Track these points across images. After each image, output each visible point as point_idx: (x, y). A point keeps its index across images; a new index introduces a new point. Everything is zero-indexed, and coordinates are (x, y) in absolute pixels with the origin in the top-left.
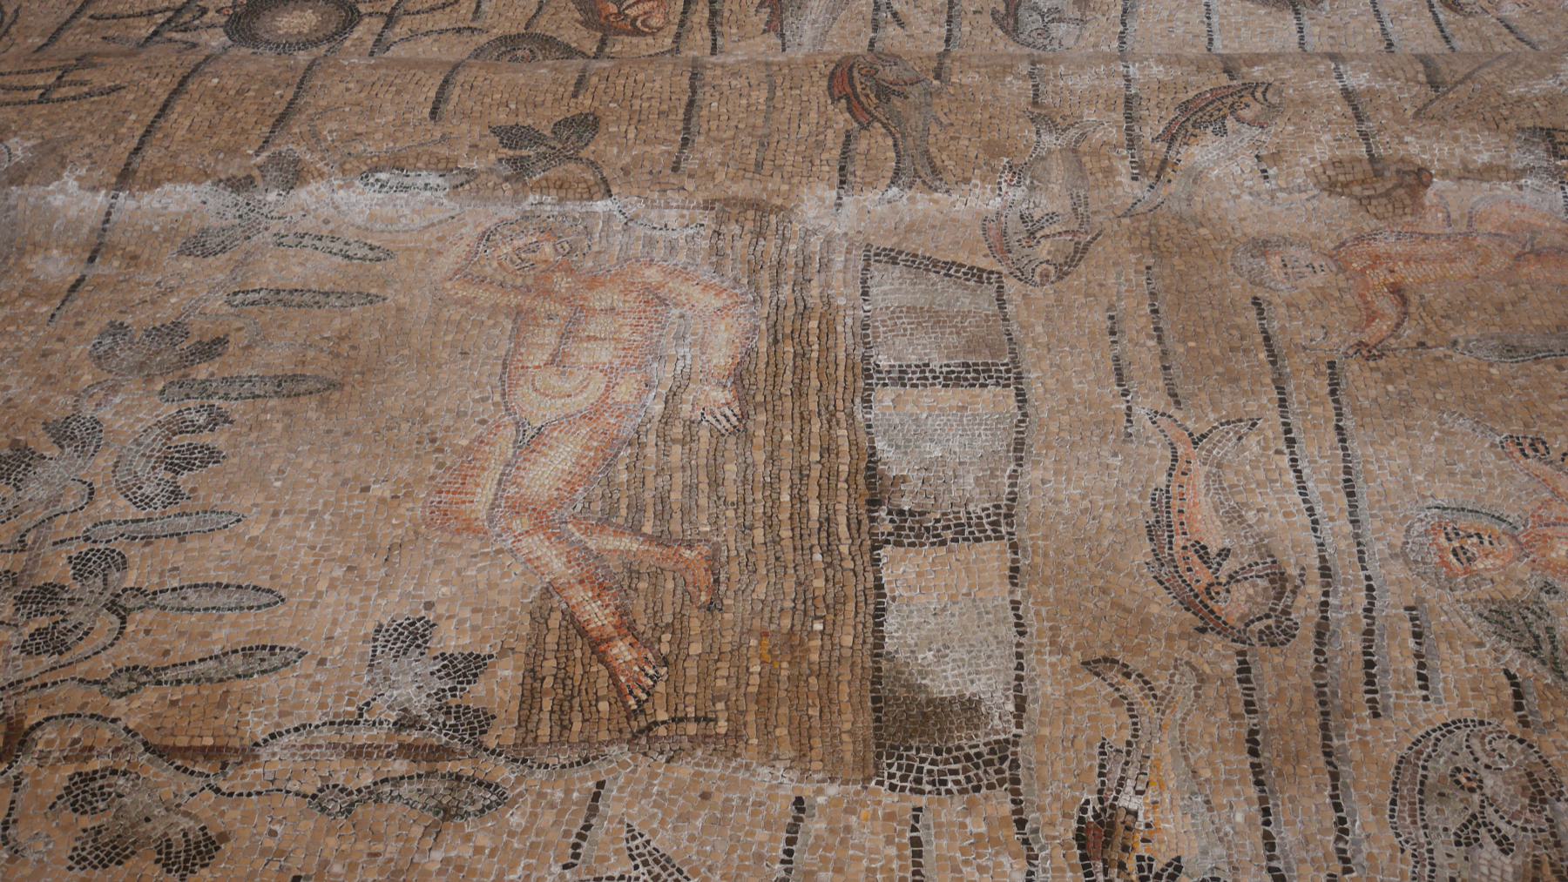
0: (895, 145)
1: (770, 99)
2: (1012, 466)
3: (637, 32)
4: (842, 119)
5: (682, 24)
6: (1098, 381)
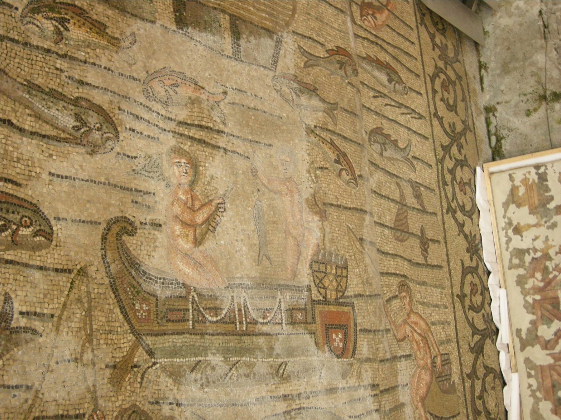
0: (320, 57)
1: (335, 28)
2: (203, 43)
3: (362, 16)
4: (330, 46)
5: (366, 30)
6: (236, 83)
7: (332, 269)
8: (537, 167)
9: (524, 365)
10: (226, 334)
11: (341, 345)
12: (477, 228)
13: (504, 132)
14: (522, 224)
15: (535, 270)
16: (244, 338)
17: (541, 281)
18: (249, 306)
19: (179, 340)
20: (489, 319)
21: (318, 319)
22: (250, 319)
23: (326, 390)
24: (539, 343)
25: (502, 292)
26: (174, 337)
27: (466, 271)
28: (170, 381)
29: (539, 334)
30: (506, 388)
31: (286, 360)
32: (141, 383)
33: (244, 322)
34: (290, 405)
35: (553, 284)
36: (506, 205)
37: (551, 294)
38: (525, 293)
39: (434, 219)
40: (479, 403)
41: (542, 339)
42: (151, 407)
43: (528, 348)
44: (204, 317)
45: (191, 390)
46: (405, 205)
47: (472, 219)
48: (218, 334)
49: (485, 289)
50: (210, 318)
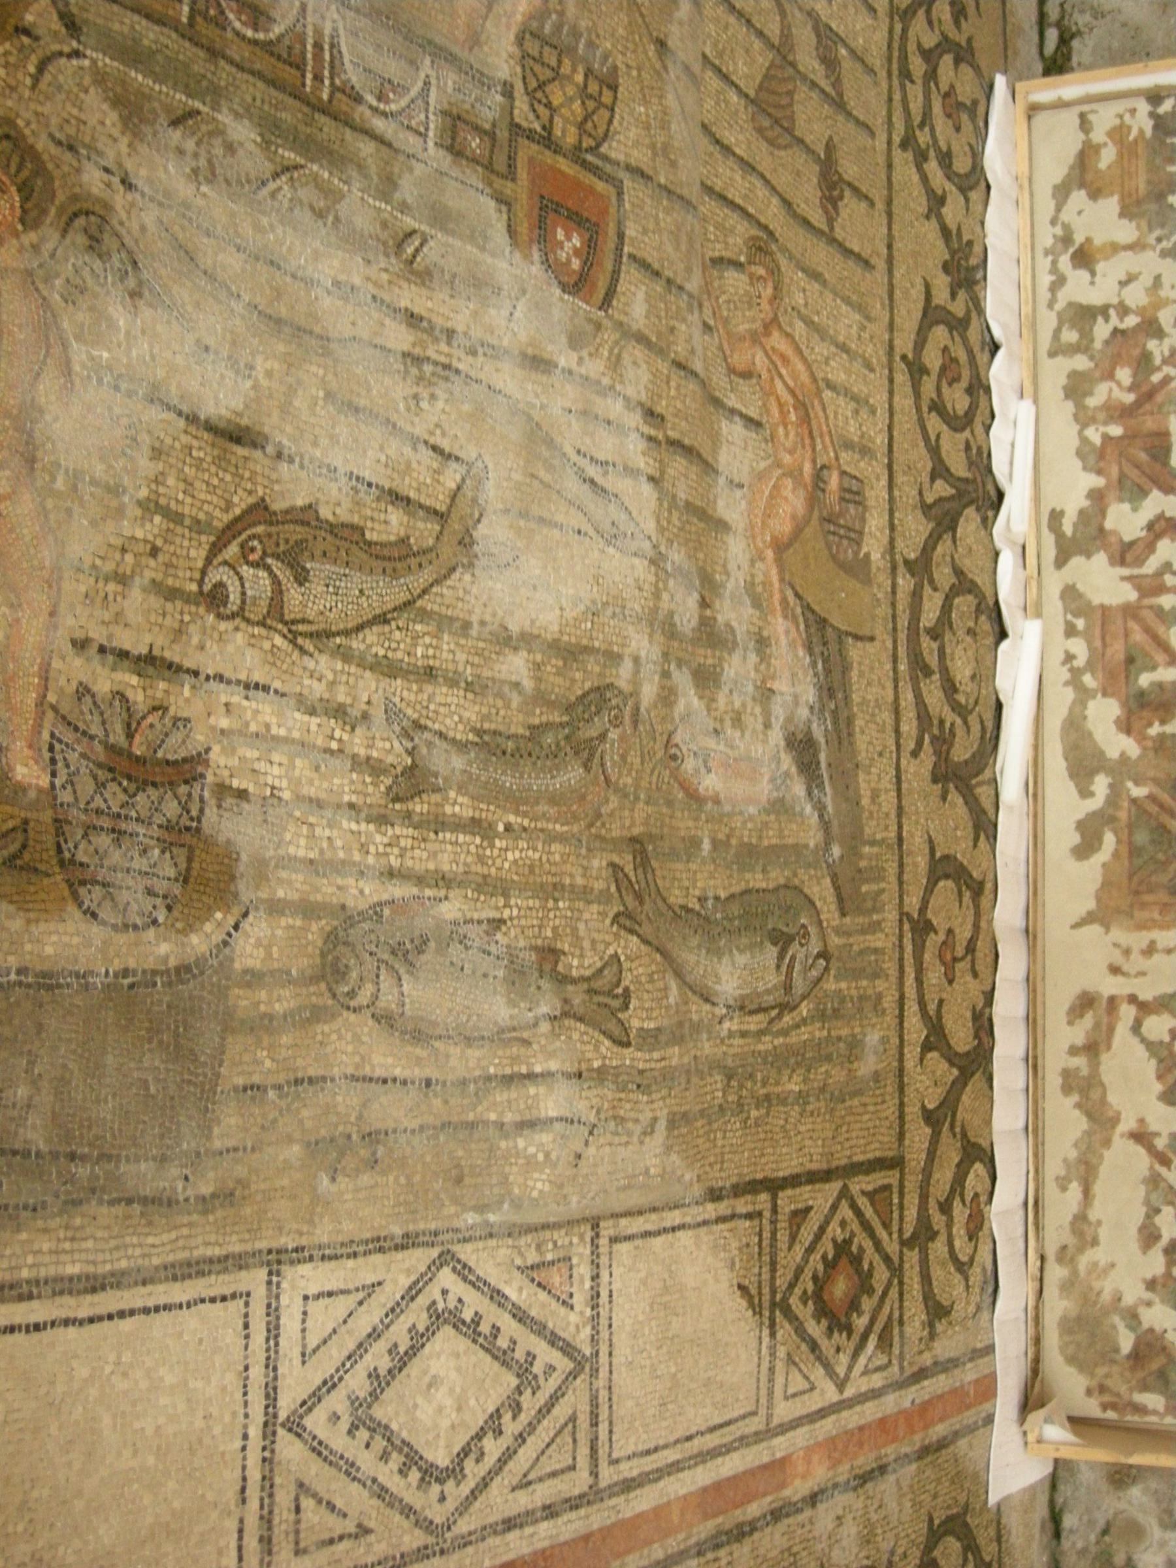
7: (574, 70)
8: (1155, 97)
9: (1059, 604)
10: (272, 83)
11: (576, 264)
12: (978, 229)
13: (1081, 20)
14: (1097, 242)
15: (1116, 360)
16: (322, 119)
17: (1130, 389)
18: (344, 49)
19: (151, 35)
20: (981, 460)
21: (522, 174)
22: (344, 83)
23: (524, 355)
24: (1105, 547)
25: (1025, 411)
26: (136, 18)
27: (932, 315)
28: (112, 117)
29: (1109, 524)
30: (1004, 646)
31: (424, 227)
32: (36, 79)
33: (327, 82)
34: (422, 344)
35: (1159, 398)
36: (1062, 192)
37: (1150, 424)
38: (1083, 419)
39: (863, 139)
40: (926, 643)
41: (1113, 539)
42: (54, 150)
43: (1077, 562)
44: (222, 13)
45: (166, 170)
46: (793, 65)
47: (967, 200)
48: (252, 73)
49: (979, 388)
50: (237, 25)
